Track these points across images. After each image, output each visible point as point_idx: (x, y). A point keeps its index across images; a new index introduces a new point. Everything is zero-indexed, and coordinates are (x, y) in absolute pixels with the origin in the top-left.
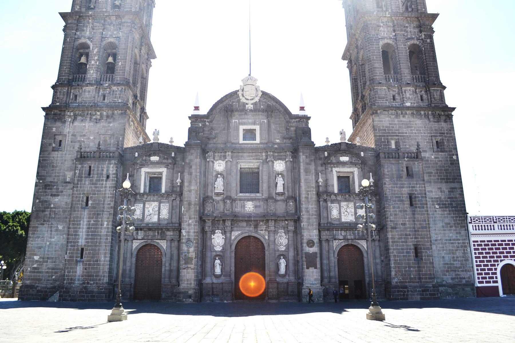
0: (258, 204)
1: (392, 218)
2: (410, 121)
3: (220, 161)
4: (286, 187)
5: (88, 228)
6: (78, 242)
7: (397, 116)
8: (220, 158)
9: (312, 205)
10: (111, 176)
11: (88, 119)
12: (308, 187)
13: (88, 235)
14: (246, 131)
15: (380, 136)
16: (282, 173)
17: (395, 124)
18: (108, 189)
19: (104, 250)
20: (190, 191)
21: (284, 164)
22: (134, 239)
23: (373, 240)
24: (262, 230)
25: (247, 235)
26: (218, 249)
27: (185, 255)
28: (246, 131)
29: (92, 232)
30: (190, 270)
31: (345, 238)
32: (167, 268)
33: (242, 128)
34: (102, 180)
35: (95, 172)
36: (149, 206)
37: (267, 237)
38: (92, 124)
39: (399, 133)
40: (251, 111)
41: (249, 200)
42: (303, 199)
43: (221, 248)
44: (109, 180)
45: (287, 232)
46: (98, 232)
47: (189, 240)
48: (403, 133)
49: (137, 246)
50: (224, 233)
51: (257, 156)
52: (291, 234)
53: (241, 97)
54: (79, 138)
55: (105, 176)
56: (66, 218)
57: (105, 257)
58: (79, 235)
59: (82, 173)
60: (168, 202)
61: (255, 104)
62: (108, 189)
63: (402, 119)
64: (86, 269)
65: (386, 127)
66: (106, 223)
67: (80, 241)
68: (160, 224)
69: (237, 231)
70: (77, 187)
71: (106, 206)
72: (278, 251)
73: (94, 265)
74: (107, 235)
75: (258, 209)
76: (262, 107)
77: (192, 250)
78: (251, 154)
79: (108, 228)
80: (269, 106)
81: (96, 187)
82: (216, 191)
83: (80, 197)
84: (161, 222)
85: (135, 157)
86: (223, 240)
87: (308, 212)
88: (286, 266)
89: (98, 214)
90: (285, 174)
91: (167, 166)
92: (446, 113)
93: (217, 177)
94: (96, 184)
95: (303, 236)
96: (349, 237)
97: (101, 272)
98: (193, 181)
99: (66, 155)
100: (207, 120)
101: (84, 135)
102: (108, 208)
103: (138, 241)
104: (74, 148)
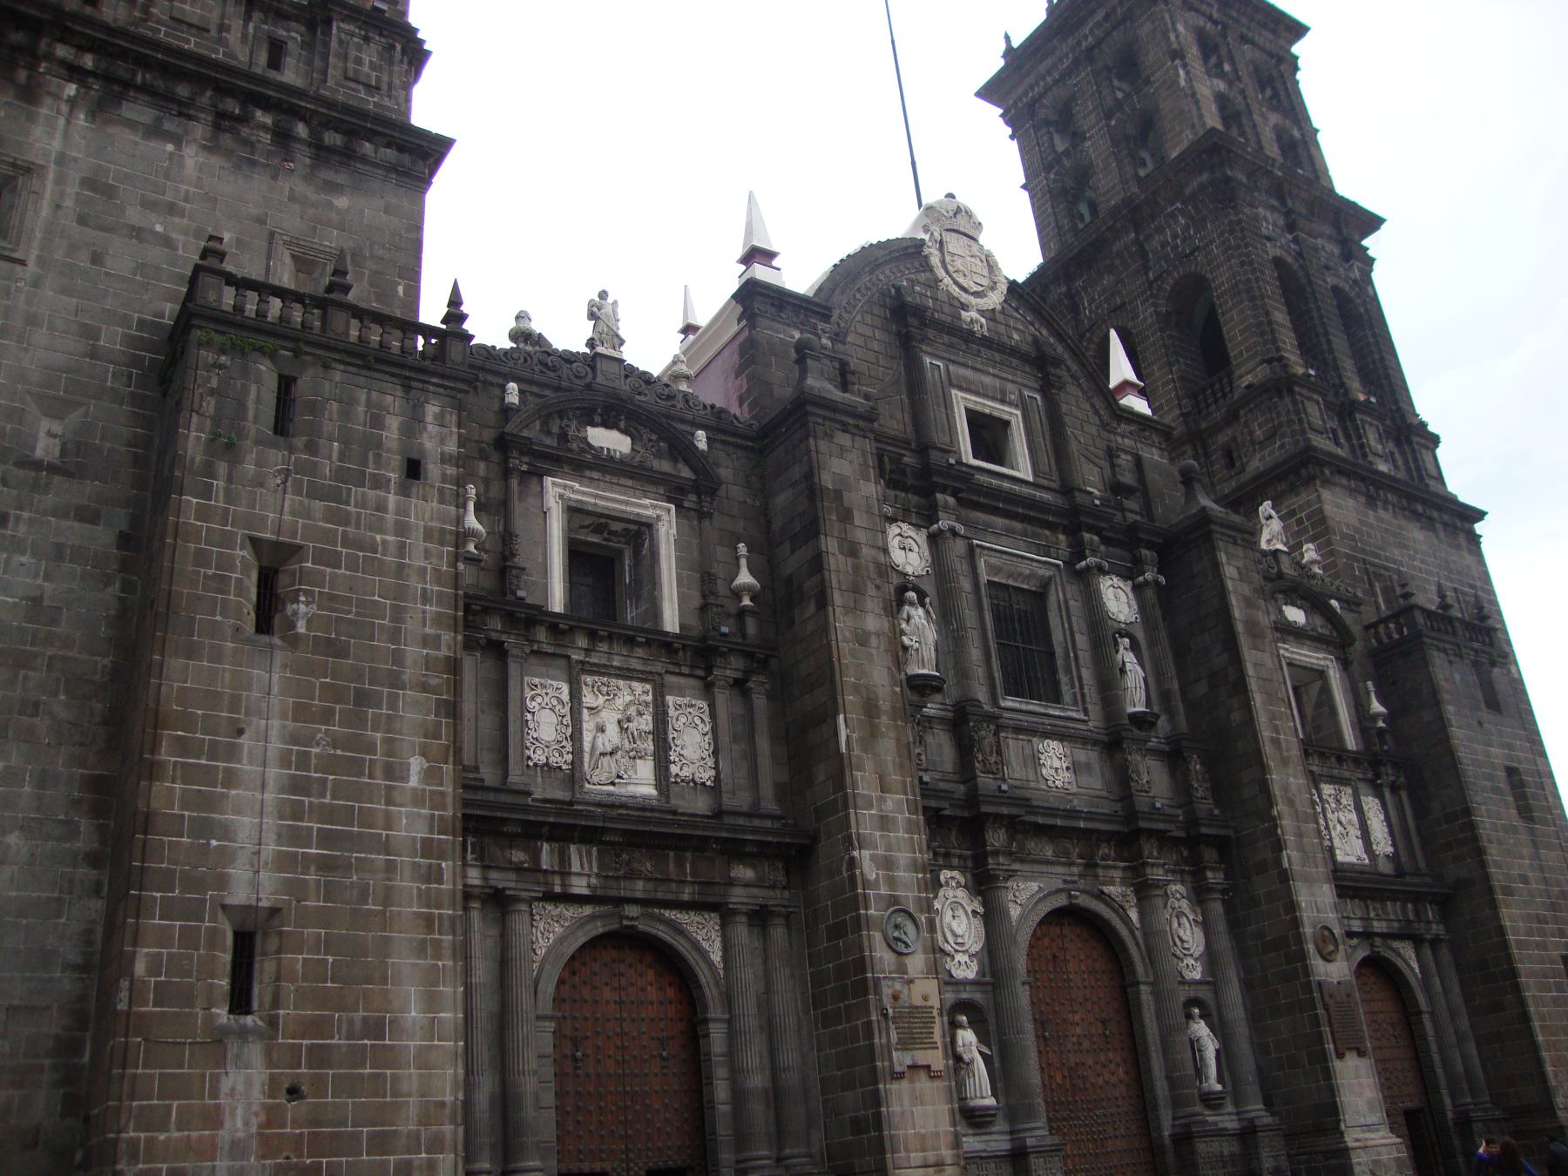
0: (1082, 755)
1: (1493, 853)
2: (1401, 528)
3: (905, 526)
4: (1153, 696)
5: (297, 786)
6: (223, 882)
7: (1371, 502)
8: (906, 510)
9: (1296, 777)
10: (433, 470)
11: (200, 130)
12: (1271, 697)
13: (296, 836)
14: (977, 420)
15: (1348, 556)
16: (1131, 629)
17: (1371, 526)
18: (417, 542)
19: (421, 949)
20: (862, 639)
21: (1131, 595)
22: (550, 897)
23: (1435, 943)
24: (1112, 883)
25: (1061, 901)
26: (965, 968)
27: (895, 997)
28: (977, 420)
29: (328, 814)
30: (923, 1083)
31: (1367, 935)
32: (757, 1081)
33: (961, 401)
34: (379, 483)
35: (329, 426)
36: (601, 700)
37: (1134, 915)
38: (216, 161)
39: (1387, 559)
40: (986, 342)
41: (1047, 735)
42: (1268, 749)
43: (975, 967)
44: (416, 488)
45: (1199, 894)
46: (367, 819)
47: (894, 900)
48: (1394, 562)
49: (561, 940)
50: (984, 885)
51: (1034, 536)
52: (1217, 908)
53: (941, 273)
54: (134, 215)
55: (396, 461)
56: (35, 708)
57: (432, 1002)
58: (226, 832)
59: (241, 407)
60: (707, 690)
61: (990, 315)
62: (417, 542)
63: (1381, 512)
64: (294, 1092)
65: (1357, 530)
66: (416, 764)
67: (239, 873)
68: (674, 813)
69: (1026, 879)
70: (207, 492)
71: (413, 651)
72: (1183, 982)
73: (357, 1057)
74: (428, 848)
75: (1085, 779)
76: (1016, 336)
77: (916, 962)
78: (1018, 526)
79: (437, 801)
80: (1036, 342)
81: (344, 519)
82: (916, 669)
83: (226, 563)
84: (675, 802)
85: (506, 411)
86: (977, 924)
87: (1291, 802)
88: (1217, 1051)
89: (363, 698)
90: (1140, 635)
91: (675, 492)
92: (1467, 525)
93: (901, 602)
94: (337, 496)
95: (1292, 907)
96: (1378, 926)
97: (413, 1112)
98: (871, 590)
99: (36, 283)
100: (821, 326)
101: (172, 209)
102: (428, 663)
103: (571, 912)
104: (97, 259)
